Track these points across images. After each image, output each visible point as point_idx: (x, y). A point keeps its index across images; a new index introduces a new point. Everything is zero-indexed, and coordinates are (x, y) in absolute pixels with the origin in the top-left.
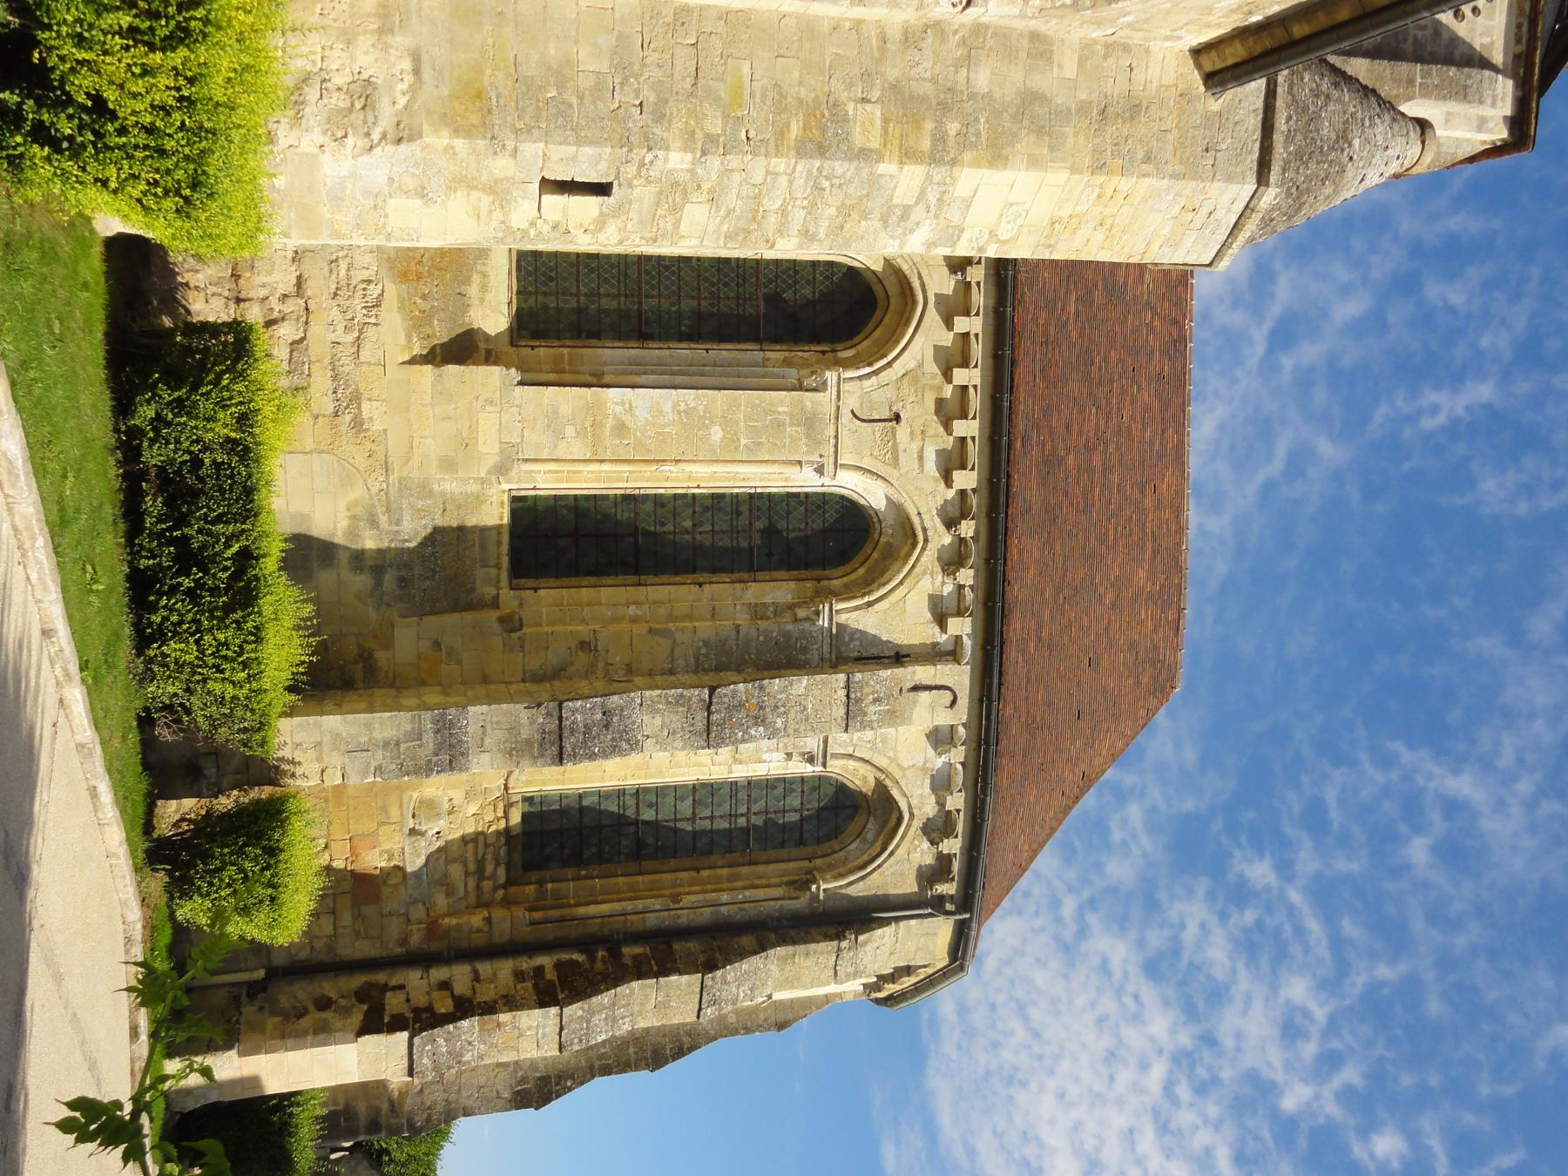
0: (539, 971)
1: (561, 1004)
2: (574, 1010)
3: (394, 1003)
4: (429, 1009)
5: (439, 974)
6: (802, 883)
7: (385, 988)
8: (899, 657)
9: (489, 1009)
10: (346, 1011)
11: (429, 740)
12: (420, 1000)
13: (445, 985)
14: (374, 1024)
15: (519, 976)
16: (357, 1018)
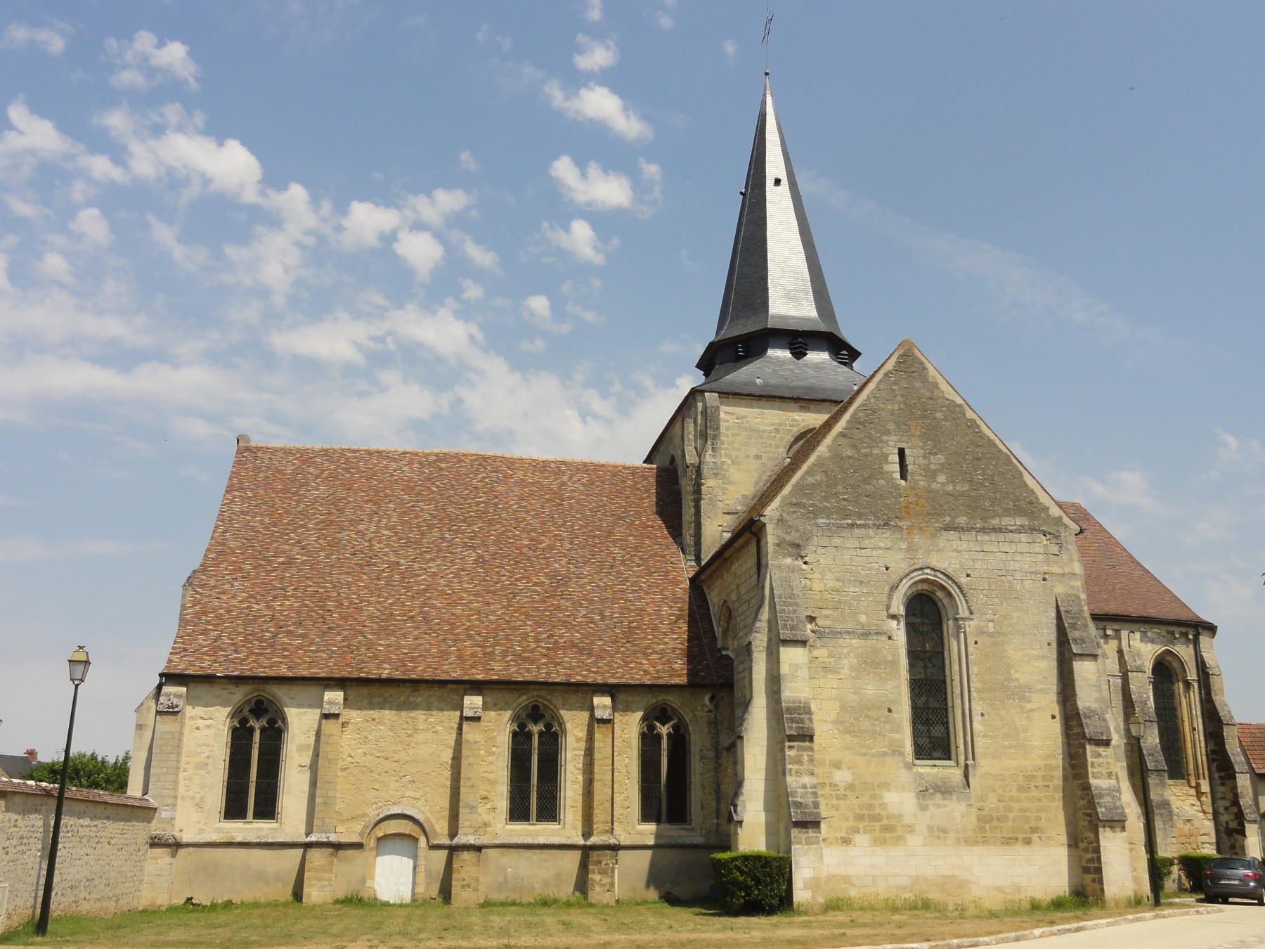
0: (1221, 778)
1: (1235, 772)
2: (1237, 768)
3: (1233, 825)
4: (1236, 814)
5: (1222, 810)
6: (1188, 685)
7: (1227, 828)
8: (1120, 651)
9: (1236, 796)
10: (1236, 841)
11: (1163, 811)
12: (1232, 817)
13: (1226, 809)
14: (1242, 833)
15: (1223, 784)
16: (1239, 837)
